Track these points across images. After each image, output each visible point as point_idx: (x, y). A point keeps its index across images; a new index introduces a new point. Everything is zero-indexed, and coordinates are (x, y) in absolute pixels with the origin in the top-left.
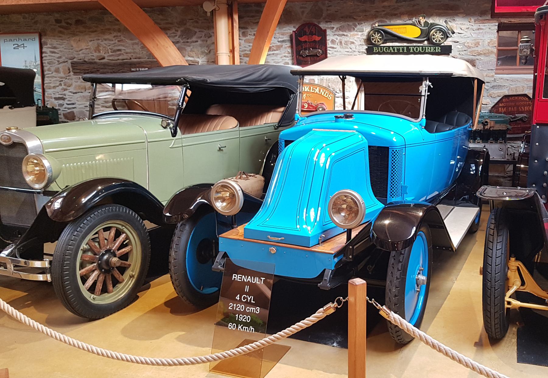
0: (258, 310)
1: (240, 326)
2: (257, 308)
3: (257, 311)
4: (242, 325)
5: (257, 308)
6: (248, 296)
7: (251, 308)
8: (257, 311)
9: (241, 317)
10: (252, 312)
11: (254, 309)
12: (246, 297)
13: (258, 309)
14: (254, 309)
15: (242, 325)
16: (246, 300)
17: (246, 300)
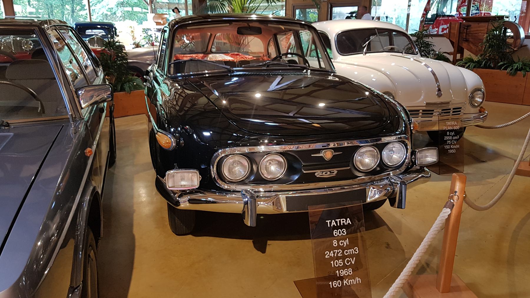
0: (357, 250)
1: (345, 281)
2: (355, 249)
3: (356, 252)
4: (347, 279)
5: (355, 249)
6: (351, 259)
7: (349, 251)
8: (356, 252)
9: (342, 272)
10: (351, 253)
11: (352, 251)
12: (349, 260)
13: (356, 249)
14: (352, 251)
15: (347, 279)
16: (350, 263)
17: (350, 263)
